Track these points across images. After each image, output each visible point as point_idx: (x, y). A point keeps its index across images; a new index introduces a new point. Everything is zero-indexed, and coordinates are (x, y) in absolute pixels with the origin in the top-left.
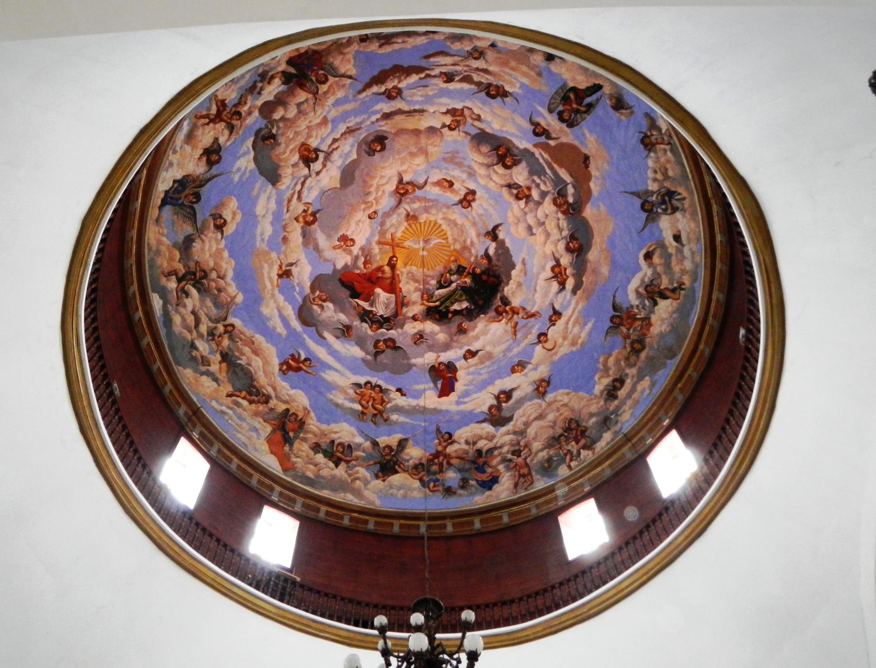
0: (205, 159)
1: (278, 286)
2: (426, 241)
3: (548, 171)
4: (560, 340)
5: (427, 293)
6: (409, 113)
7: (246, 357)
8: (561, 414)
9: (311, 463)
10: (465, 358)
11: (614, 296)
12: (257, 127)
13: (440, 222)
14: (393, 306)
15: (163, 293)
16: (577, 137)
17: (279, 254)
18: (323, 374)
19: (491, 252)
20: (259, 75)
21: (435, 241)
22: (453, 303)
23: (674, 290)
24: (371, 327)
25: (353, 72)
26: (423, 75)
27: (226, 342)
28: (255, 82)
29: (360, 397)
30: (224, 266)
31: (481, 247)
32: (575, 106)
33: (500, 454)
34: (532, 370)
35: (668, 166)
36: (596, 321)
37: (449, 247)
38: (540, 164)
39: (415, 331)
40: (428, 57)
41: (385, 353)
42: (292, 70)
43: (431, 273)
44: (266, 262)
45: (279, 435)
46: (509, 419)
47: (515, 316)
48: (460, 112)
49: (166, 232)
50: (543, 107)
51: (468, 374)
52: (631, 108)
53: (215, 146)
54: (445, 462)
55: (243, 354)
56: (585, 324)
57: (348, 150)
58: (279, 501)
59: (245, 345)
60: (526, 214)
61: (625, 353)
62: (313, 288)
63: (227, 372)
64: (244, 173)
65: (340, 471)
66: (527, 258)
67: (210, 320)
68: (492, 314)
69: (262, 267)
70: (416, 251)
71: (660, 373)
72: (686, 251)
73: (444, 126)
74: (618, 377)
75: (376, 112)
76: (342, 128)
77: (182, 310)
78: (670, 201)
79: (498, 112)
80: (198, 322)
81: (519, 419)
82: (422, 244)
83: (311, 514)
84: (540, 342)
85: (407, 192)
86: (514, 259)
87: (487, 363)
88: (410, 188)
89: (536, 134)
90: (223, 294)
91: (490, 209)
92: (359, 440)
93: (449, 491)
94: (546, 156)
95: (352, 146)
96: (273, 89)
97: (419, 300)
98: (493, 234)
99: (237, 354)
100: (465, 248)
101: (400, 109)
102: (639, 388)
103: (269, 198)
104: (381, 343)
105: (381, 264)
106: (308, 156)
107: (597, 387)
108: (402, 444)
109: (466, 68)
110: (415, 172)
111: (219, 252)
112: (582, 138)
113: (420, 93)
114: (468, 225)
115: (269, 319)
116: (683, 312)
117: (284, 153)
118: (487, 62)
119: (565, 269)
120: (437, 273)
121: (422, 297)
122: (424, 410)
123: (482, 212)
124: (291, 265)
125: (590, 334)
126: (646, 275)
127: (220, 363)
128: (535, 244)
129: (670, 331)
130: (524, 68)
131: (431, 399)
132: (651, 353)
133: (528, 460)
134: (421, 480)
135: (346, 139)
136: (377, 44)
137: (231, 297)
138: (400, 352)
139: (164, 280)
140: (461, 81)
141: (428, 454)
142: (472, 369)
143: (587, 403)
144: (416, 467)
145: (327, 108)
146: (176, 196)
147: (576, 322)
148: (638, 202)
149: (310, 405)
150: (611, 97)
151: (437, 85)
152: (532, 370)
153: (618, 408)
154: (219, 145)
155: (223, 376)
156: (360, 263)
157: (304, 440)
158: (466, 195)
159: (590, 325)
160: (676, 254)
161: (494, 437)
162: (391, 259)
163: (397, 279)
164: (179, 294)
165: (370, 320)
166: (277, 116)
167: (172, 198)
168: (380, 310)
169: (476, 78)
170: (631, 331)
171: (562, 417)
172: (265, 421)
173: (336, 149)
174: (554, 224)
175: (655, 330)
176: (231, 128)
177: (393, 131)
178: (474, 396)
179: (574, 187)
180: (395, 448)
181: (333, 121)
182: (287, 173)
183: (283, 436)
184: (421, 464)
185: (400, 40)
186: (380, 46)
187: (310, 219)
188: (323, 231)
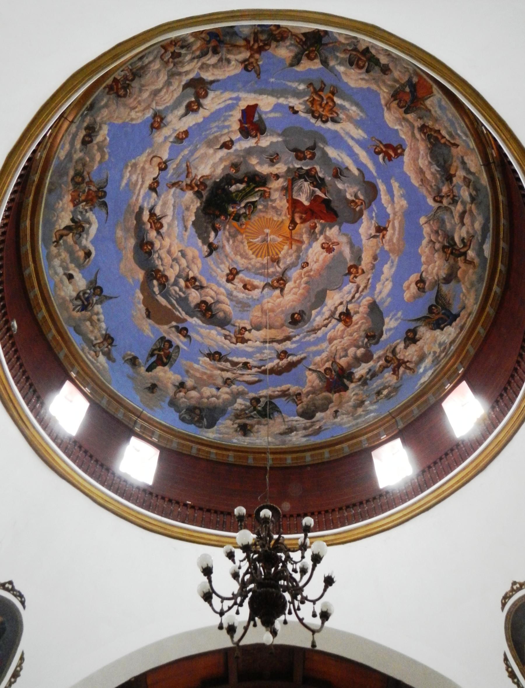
0: (417, 336)
1: (389, 222)
2: (264, 240)
3: (174, 302)
4: (147, 166)
5: (266, 198)
6: (272, 341)
7: (431, 171)
10: (232, 142)
13: (253, 256)
14: (296, 188)
15: (480, 252)
16: (158, 330)
18: (366, 137)
19: (213, 234)
22: (244, 189)
23: (61, 236)
25: (308, 373)
26: (263, 368)
27: (445, 189)
28: (371, 379)
29: (335, 109)
30: (427, 250)
31: (221, 238)
32: (162, 353)
33: (193, 53)
34: (170, 136)
35: (91, 328)
37: (246, 236)
38: (181, 307)
39: (277, 166)
40: (259, 381)
41: (306, 149)
43: (262, 214)
44: (394, 244)
45: (420, 93)
46: (185, 87)
48: (239, 340)
51: (228, 127)
52: (125, 361)
54: (252, 42)
55: (432, 173)
56: (127, 185)
57: (318, 318)
59: (429, 181)
60: (188, 267)
61: (87, 169)
62: (361, 213)
63: (451, 165)
66: (184, 232)
68: (209, 183)
69: (398, 240)
70: (273, 233)
72: (60, 271)
73: (250, 331)
74: (89, 145)
76: (320, 334)
77: (471, 231)
78: (83, 302)
81: (177, 85)
84: (165, 163)
87: (211, 137)
88: (276, 284)
89: (186, 329)
90: (435, 228)
91: (214, 267)
92: (341, 69)
94: (177, 313)
95: (314, 320)
96: (361, 371)
97: (272, 191)
98: (212, 248)
99: (438, 176)
101: (279, 344)
102: (67, 147)
103: (380, 292)
104: (308, 157)
105: (302, 225)
106: (346, 317)
107: (106, 132)
109: (235, 371)
110: (271, 296)
111: (428, 263)
112: (152, 328)
113: (265, 355)
114: (232, 255)
115: (402, 196)
116: (49, 223)
117: (362, 323)
119: (151, 227)
121: (270, 194)
122: (272, 93)
124: (375, 237)
125: (122, 177)
126: (87, 239)
127: (454, 175)
128: (178, 244)
130: (198, 375)
131: (266, 103)
132: (65, 179)
135: (318, 326)
136: (290, 391)
138: (292, 146)
139: (477, 261)
142: (226, 131)
145: (328, 350)
147: (136, 184)
148: (106, 292)
149: (383, 110)
150: (140, 366)
151: (254, 361)
152: (170, 136)
155: (456, 163)
157: (396, 81)
158: (233, 279)
159: (123, 184)
160: (67, 264)
161: (201, 68)
162: (294, 228)
164: (468, 244)
165: (317, 181)
166: (362, 350)
167: (449, 317)
168: (307, 186)
169: (228, 365)
170: (87, 190)
174: (166, 261)
175: (68, 198)
176: (394, 352)
177: (285, 328)
178: (222, 106)
179: (154, 292)
180: (304, 58)
182: (363, 309)
183: (415, 90)
184: (278, 41)
185: (277, 393)
186: (289, 389)
187: (353, 270)
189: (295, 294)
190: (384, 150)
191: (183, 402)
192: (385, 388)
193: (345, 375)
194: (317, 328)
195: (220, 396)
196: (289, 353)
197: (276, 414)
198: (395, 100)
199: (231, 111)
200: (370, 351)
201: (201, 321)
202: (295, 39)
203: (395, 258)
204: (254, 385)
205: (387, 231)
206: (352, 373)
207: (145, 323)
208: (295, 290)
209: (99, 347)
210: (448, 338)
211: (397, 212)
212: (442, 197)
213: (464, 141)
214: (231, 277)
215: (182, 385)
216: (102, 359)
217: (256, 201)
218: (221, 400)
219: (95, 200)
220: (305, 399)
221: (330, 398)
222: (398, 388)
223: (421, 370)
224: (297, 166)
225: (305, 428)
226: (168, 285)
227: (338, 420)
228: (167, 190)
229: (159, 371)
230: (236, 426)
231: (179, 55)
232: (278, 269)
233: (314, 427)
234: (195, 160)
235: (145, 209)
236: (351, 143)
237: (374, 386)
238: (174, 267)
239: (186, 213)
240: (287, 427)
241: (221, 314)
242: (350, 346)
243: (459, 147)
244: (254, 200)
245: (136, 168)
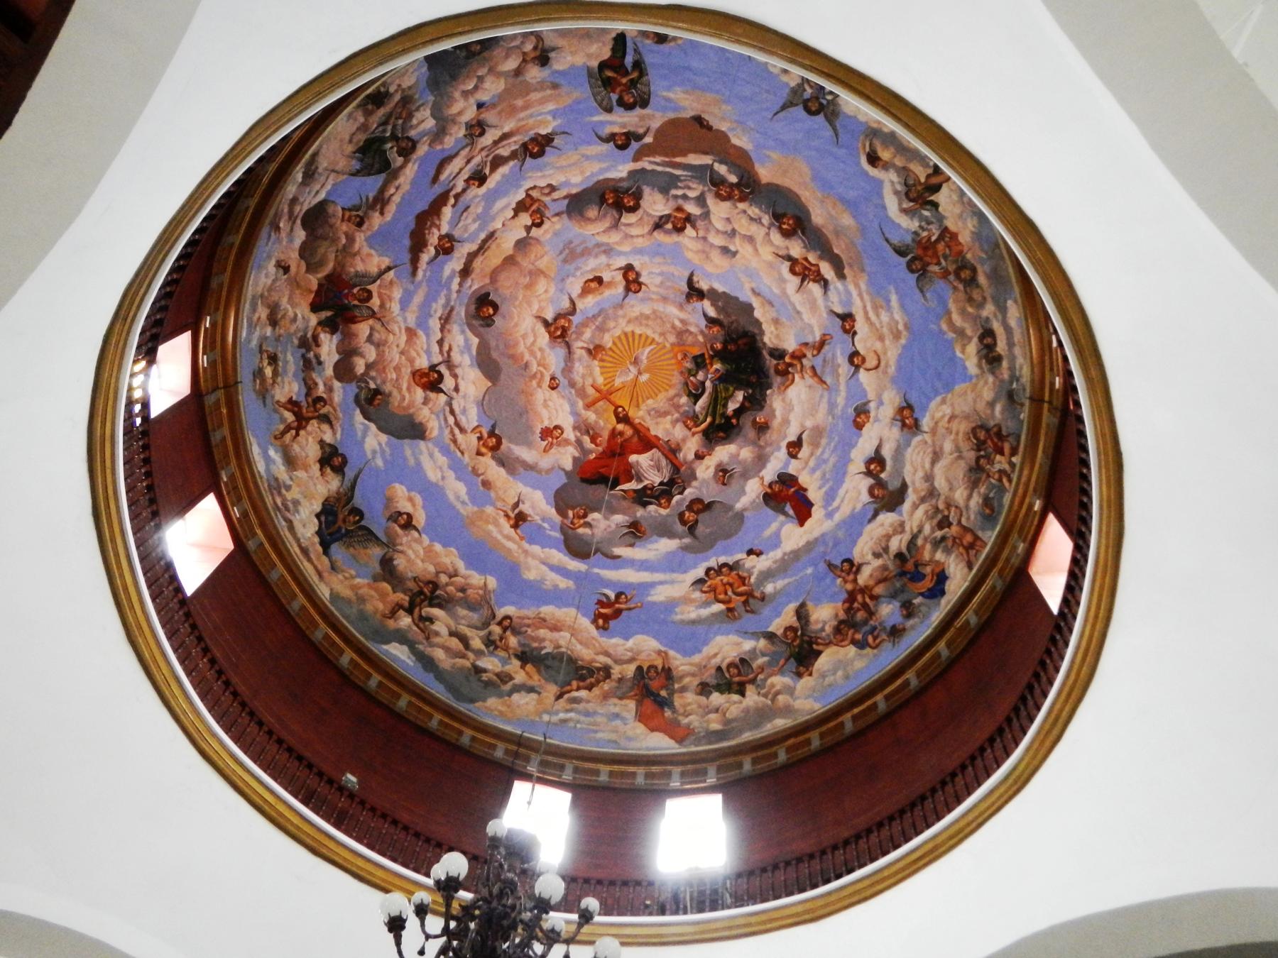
0: (328, 470)
1: (522, 538)
2: (636, 362)
3: (678, 172)
4: (878, 346)
6: (482, 248)
7: (549, 641)
8: (957, 434)
9: (710, 712)
11: (887, 240)
12: (351, 399)
13: (629, 329)
14: (664, 462)
16: (664, 109)
17: (493, 504)
18: (650, 599)
19: (712, 313)
20: (300, 346)
21: (644, 354)
22: (725, 406)
24: (660, 505)
25: (386, 262)
26: (452, 201)
27: (513, 641)
28: (303, 356)
29: (712, 595)
30: (446, 560)
31: (696, 316)
32: (624, 80)
33: (926, 539)
36: (897, 289)
39: (712, 470)
40: (435, 179)
43: (672, 392)
44: (487, 522)
45: (649, 705)
46: (904, 487)
47: (805, 361)
48: (528, 201)
49: (353, 572)
50: (600, 114)
51: (813, 470)
53: (328, 450)
54: (868, 600)
55: (543, 640)
56: (888, 301)
57: (462, 341)
59: (538, 628)
60: (705, 239)
61: (961, 295)
62: (561, 511)
63: (539, 672)
64: (383, 452)
65: (752, 698)
66: (754, 285)
67: (477, 628)
69: (489, 533)
73: (528, 229)
74: (981, 331)
75: (451, 278)
76: (435, 324)
77: (437, 640)
79: (564, 163)
80: (464, 640)
82: (634, 370)
83: (733, 774)
84: (857, 367)
85: (565, 330)
87: (824, 441)
88: (562, 322)
90: (470, 592)
91: (665, 269)
92: (748, 645)
93: (896, 632)
94: (658, 159)
95: (463, 332)
96: (329, 348)
97: (688, 433)
98: (694, 292)
99: (535, 645)
100: (680, 334)
101: (469, 254)
103: (431, 455)
105: (610, 427)
106: (431, 381)
107: (968, 364)
108: (801, 613)
109: (484, 153)
110: (551, 301)
111: (429, 550)
113: (469, 221)
114: (660, 307)
119: (806, 259)
120: (680, 386)
121: (687, 426)
122: (796, 555)
124: (516, 505)
126: (892, 182)
127: (523, 667)
128: (748, 262)
130: (535, 96)
131: (793, 536)
132: (987, 268)
134: (854, 642)
136: (377, 214)
138: (717, 508)
139: (391, 624)
140: (493, 169)
141: (840, 604)
144: (837, 630)
145: (400, 319)
147: (876, 308)
148: (799, 111)
151: (475, 197)
152: (878, 408)
153: (1012, 368)
154: (330, 445)
155: (536, 680)
156: (588, 443)
157: (683, 689)
158: (625, 276)
159: (894, 298)
161: (902, 524)
162: (616, 414)
163: (642, 430)
167: (330, 534)
168: (655, 478)
169: (504, 152)
171: (961, 435)
172: (621, 698)
174: (744, 221)
176: (326, 419)
177: (487, 281)
178: (841, 492)
179: (721, 162)
180: (796, 624)
183: (655, 701)
184: (841, 622)
185: (392, 190)
186: (382, 213)
187: (492, 442)
189: (524, 336)
192: (275, 373)
194: (448, 327)
196: (441, 257)
197: (356, 165)
199: (826, 493)
203: (467, 510)
204: (435, 167)
207: (695, 105)
210: (301, 521)
212: (505, 630)
213: (557, 713)
215: (543, 59)
217: (695, 404)
218: (457, 95)
220: (344, 227)
221: (317, 272)
222: (264, 398)
223: (272, 453)
224: (686, 492)
225: (294, 201)
227: (271, 268)
230: (392, 89)
231: (941, 526)
233: (286, 217)
234: (822, 396)
235: (835, 279)
236: (658, 577)
237: (290, 357)
238: (723, 222)
240: (320, 170)
241: (592, 212)
242: (380, 355)
244: (702, 402)
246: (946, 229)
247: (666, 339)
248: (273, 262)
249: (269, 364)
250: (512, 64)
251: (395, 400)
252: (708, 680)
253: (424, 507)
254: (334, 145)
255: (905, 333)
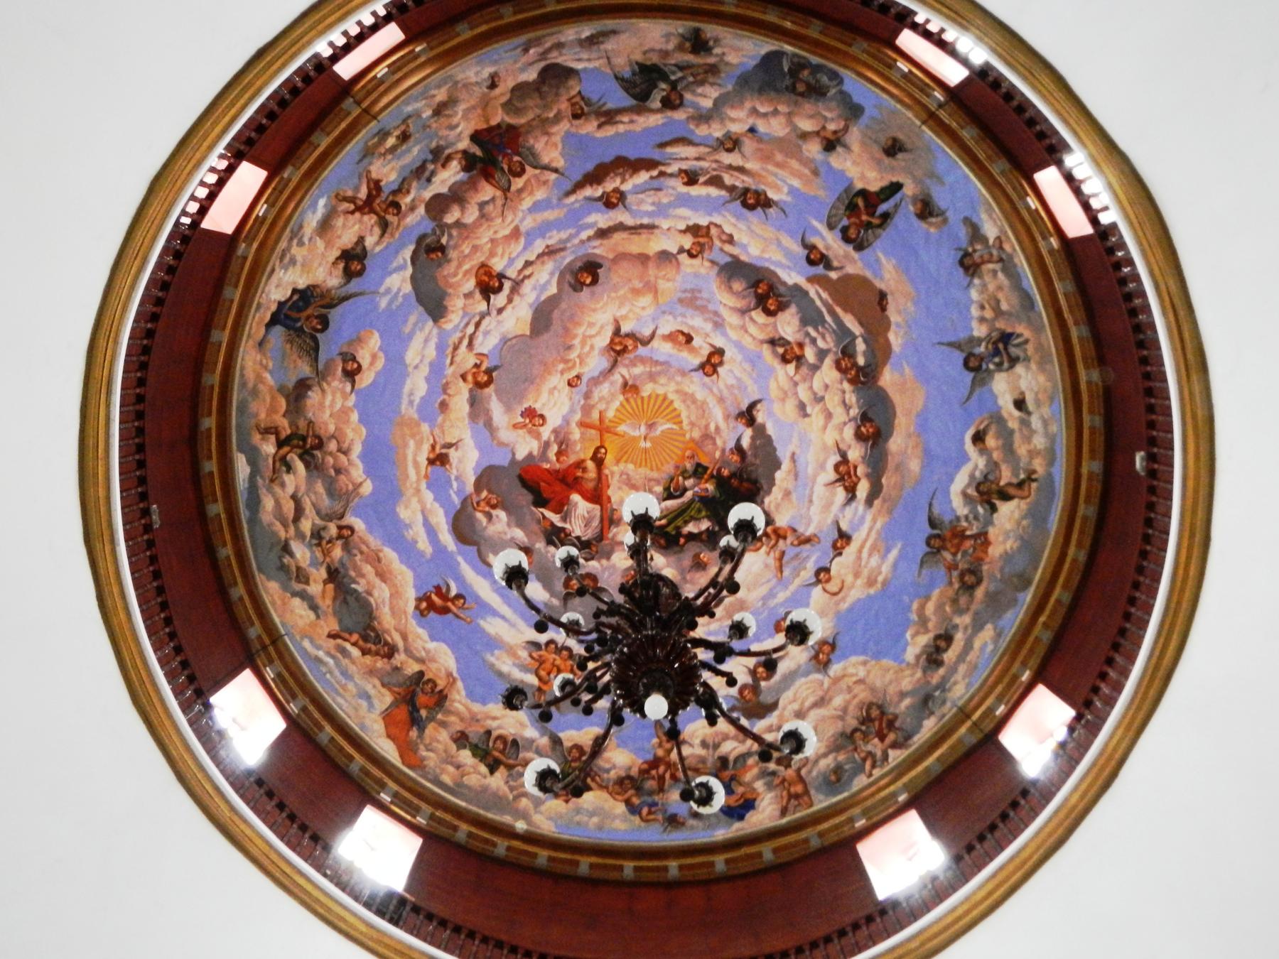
0: (341, 265)
1: (426, 476)
2: (651, 426)
3: (828, 318)
4: (849, 579)
7: (366, 580)
8: (855, 697)
9: (452, 764)
11: (930, 505)
13: (671, 396)
14: (596, 523)
16: (868, 265)
17: (432, 427)
18: (482, 623)
19: (745, 443)
20: (431, 152)
21: (663, 426)
22: (686, 523)
23: (1020, 485)
25: (560, 163)
26: (655, 173)
27: (337, 552)
28: (425, 162)
30: (350, 434)
32: (864, 218)
35: (1000, 296)
37: (684, 435)
40: (663, 145)
42: (477, 151)
43: (655, 475)
44: (413, 436)
45: (403, 713)
46: (773, 706)
47: (781, 542)
49: (271, 365)
50: (821, 221)
52: (942, 213)
53: (359, 250)
54: (667, 776)
55: (363, 576)
56: (888, 550)
57: (545, 280)
58: (392, 802)
59: (367, 561)
60: (796, 384)
61: (951, 593)
62: (478, 485)
63: (335, 599)
65: (497, 781)
66: (798, 452)
67: (318, 513)
69: (406, 445)
70: (635, 440)
71: (1009, 615)
72: (1035, 422)
73: (681, 250)
74: (942, 632)
75: (589, 226)
76: (539, 246)
77: (277, 489)
78: (1006, 349)
79: (759, 231)
80: (299, 512)
84: (819, 581)
85: (625, 350)
86: (779, 453)
88: (630, 343)
89: (811, 262)
90: (342, 477)
91: (745, 378)
94: (825, 295)
95: (552, 274)
98: (748, 416)
99: (353, 574)
100: (707, 436)
101: (621, 224)
102: (977, 644)
103: (426, 341)
105: (582, 456)
106: (489, 284)
109: (714, 165)
111: (345, 411)
112: (876, 267)
113: (650, 200)
114: (712, 402)
115: (408, 526)
116: (1037, 516)
117: (455, 275)
118: (743, 156)
119: (855, 467)
120: (665, 476)
123: (734, 382)
124: (449, 446)
125: (895, 566)
126: (976, 467)
127: (325, 582)
128: (810, 431)
129: (1019, 549)
130: (794, 164)
132: (992, 588)
133: (803, 772)
134: (628, 802)
135: (543, 263)
136: (595, 124)
137: (353, 484)
139: (256, 438)
140: (707, 183)
141: (640, 761)
143: (892, 675)
144: (620, 782)
145: (520, 214)
146: (294, 315)
147: (874, 548)
148: (959, 357)
149: (459, 670)
150: (915, 200)
151: (673, 188)
154: (364, 248)
155: (326, 604)
156: (552, 454)
157: (443, 724)
158: (711, 355)
159: (894, 553)
160: (1021, 430)
162: (597, 450)
164: (278, 464)
166: (450, 219)
167: (287, 316)
169: (728, 179)
170: (959, 556)
171: (855, 702)
172: (383, 685)
173: (529, 277)
174: (837, 399)
175: (995, 551)
176: (384, 226)
177: (611, 256)
179: (865, 341)
180: (588, 750)
181: (528, 234)
182: (456, 305)
183: (411, 713)
184: (629, 777)
185: (626, 119)
186: (600, 126)
187: (482, 379)
188: (500, 399)
189: (591, 325)
190: (450, 604)
191: (830, 110)
192: (393, 149)
193: (479, 166)
195: (748, 116)
196: (600, 204)
197: (627, 73)
198: (441, 691)
200: (434, 219)
201: (778, 277)
202: (603, 780)
204: (675, 135)
205: (428, 459)
206: (466, 168)
207: (892, 282)
208: (593, 331)
209: (991, 255)
211: (414, 495)
213: (319, 648)
214: (715, 360)
215: (830, 145)
216: (990, 230)
218: (748, 105)
219: (947, 534)
220: (564, 106)
222: (364, 156)
224: (593, 563)
225: (559, 46)
226: (836, 353)
227: (487, 71)
228: (821, 531)
229: (876, 179)
230: (717, 51)
232: (624, 371)
233: (540, 50)
234: (769, 581)
237: (415, 150)
239: (790, 486)
240: (602, 47)
242: (477, 224)
243: (326, 633)
245: (869, 578)
246: (986, 533)
247: (691, 430)
248: (491, 69)
249: (398, 137)
250: (806, 125)
251: (449, 269)
252: (471, 735)
253: (378, 374)
254: (634, 42)
255: (879, 586)
